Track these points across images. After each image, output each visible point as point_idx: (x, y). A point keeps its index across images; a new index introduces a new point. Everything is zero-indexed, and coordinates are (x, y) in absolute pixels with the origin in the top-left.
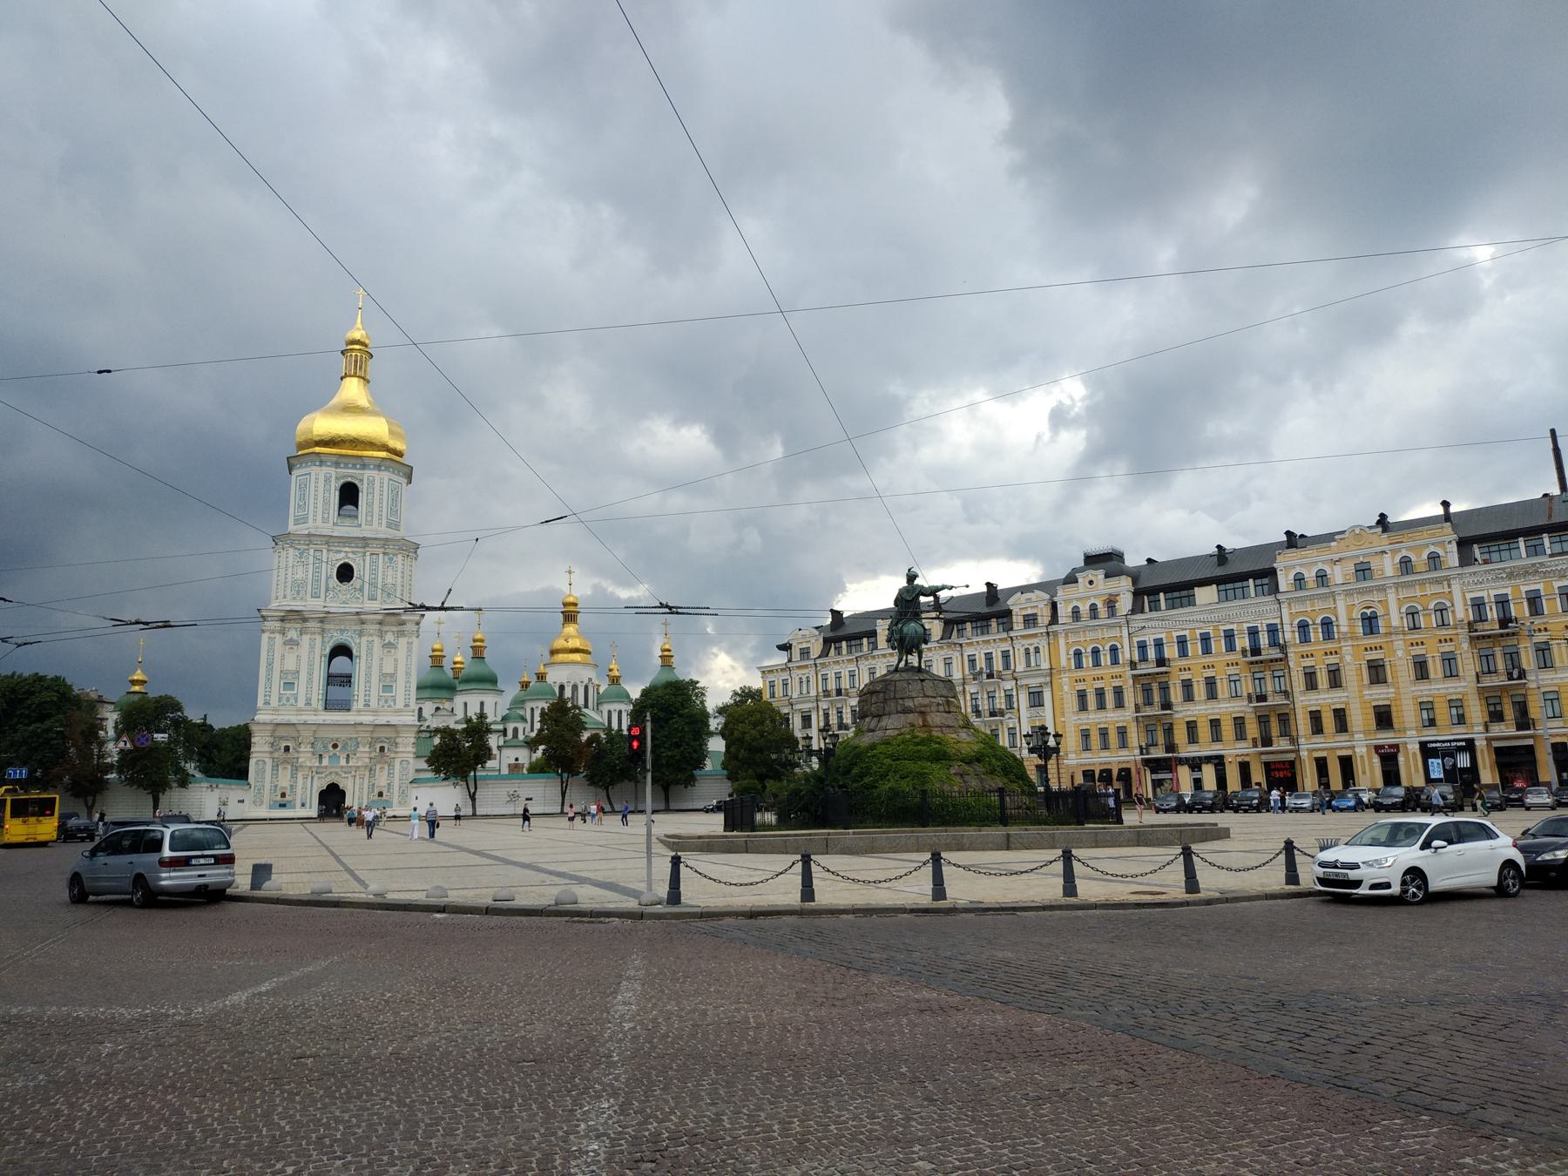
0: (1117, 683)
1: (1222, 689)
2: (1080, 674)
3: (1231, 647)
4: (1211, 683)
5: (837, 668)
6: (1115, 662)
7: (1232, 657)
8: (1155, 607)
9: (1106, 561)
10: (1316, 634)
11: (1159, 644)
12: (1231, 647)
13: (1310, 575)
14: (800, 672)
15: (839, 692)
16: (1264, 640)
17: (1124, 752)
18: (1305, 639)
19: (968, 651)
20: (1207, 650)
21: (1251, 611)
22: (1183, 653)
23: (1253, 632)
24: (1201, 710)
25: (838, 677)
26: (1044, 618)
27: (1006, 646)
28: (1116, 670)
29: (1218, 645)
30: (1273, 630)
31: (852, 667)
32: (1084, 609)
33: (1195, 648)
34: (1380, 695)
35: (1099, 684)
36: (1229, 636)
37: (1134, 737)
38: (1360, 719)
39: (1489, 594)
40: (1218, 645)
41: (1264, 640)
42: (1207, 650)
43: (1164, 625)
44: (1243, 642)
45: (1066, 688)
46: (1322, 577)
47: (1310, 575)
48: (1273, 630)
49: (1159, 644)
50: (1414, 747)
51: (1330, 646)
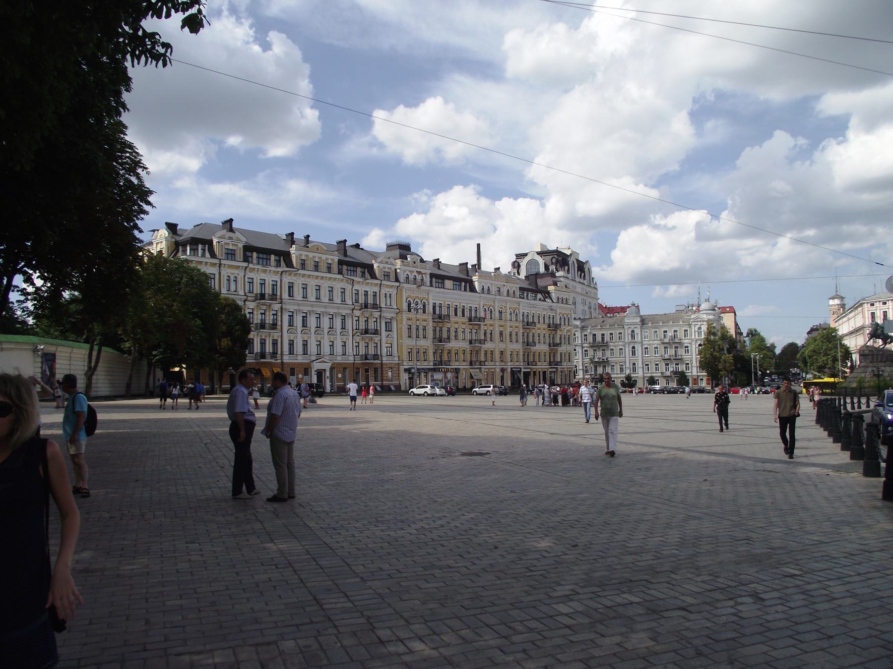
0: (424, 324)
2: (410, 315)
3: (463, 315)
5: (263, 276)
6: (424, 312)
12: (463, 315)
17: (426, 363)
19: (356, 287)
24: (453, 345)
25: (263, 284)
27: (377, 289)
28: (425, 317)
29: (459, 313)
31: (277, 278)
37: (431, 357)
38: (497, 356)
39: (526, 312)
42: (456, 315)
45: (404, 323)
50: (509, 370)
51: (491, 322)
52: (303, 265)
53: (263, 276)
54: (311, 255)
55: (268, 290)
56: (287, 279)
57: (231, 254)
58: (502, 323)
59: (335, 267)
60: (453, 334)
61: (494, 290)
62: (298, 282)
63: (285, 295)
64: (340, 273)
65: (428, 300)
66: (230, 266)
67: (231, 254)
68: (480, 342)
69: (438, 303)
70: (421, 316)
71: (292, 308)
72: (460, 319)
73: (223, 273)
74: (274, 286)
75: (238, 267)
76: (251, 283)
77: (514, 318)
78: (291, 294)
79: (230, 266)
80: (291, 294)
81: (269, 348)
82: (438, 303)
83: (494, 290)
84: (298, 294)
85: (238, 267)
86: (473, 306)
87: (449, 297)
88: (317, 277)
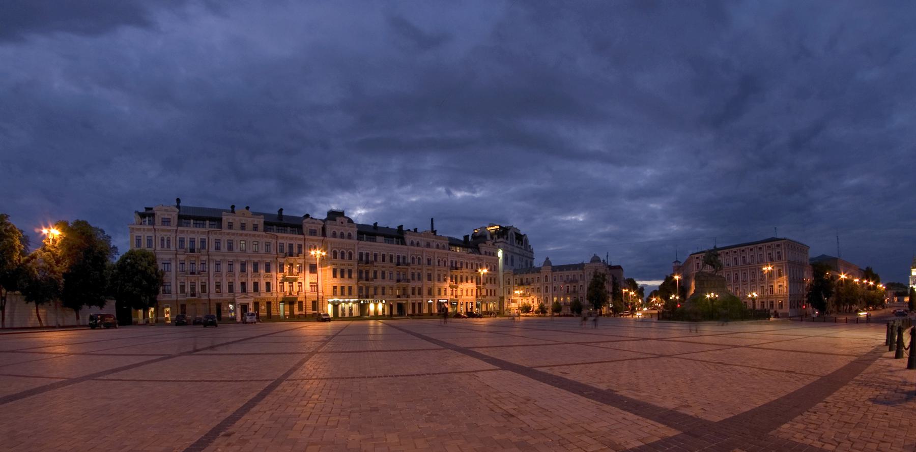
1: (387, 274)
3: (391, 261)
6: (350, 258)
7: (391, 265)
10: (416, 261)
11: (367, 255)
12: (391, 261)
13: (415, 242)
14: (163, 234)
15: (192, 250)
16: (401, 260)
18: (413, 263)
19: (280, 241)
20: (384, 260)
21: (395, 249)
22: (376, 259)
23: (398, 257)
28: (351, 262)
29: (387, 259)
30: (404, 258)
32: (338, 233)
33: (379, 258)
34: (430, 284)
35: (343, 267)
36: (391, 257)
40: (387, 259)
41: (401, 260)
42: (384, 260)
43: (367, 247)
44: (395, 260)
46: (418, 244)
47: (415, 242)
48: (404, 258)
52: (230, 226)
53: (192, 236)
54: (237, 219)
55: (198, 245)
56: (213, 237)
57: (166, 222)
58: (430, 267)
59: (261, 227)
60: (379, 275)
61: (423, 244)
62: (224, 240)
63: (212, 249)
64: (265, 231)
65: (354, 250)
66: (162, 230)
67: (166, 222)
68: (408, 281)
69: (364, 252)
70: (346, 261)
71: (218, 259)
72: (387, 263)
73: (158, 235)
74: (203, 241)
75: (169, 231)
76: (182, 241)
77: (442, 263)
78: (218, 248)
79: (162, 230)
80: (218, 248)
81: (198, 289)
82: (364, 252)
83: (423, 244)
84: (224, 247)
85: (169, 231)
86: (401, 255)
87: (380, 246)
88: (254, 235)
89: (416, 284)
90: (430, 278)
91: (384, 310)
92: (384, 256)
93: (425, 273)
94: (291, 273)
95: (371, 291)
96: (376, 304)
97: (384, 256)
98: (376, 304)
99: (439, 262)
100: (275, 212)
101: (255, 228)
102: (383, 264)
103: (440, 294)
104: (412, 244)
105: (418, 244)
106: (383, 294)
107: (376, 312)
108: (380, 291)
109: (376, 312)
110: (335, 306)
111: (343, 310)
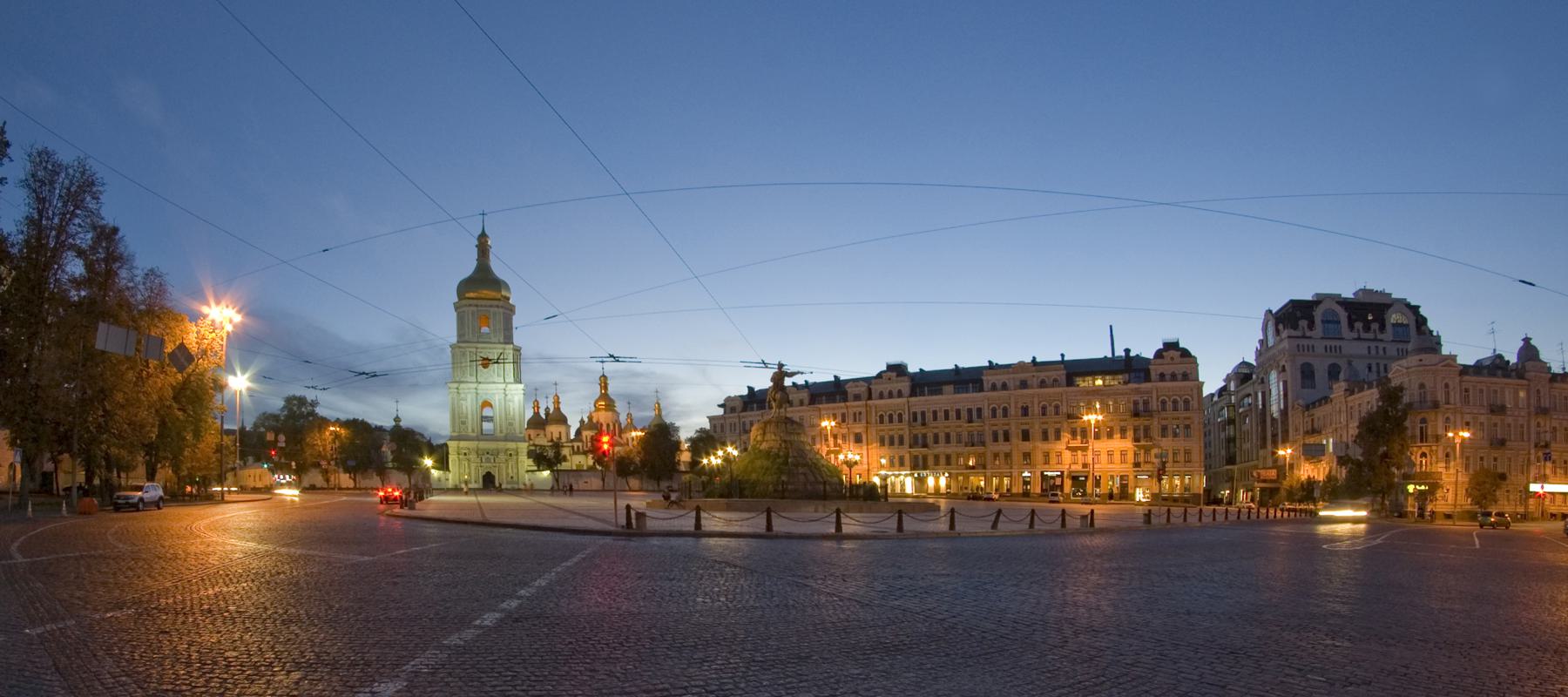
4: (948, 436)
8: (922, 394)
9: (897, 369)
11: (923, 414)
12: (958, 417)
22: (935, 418)
26: (865, 395)
29: (952, 414)
34: (1027, 446)
40: (952, 414)
43: (923, 403)
44: (964, 414)
49: (923, 414)
61: (1011, 384)
70: (896, 425)
89: (1002, 447)
90: (1026, 436)
91: (948, 487)
92: (946, 412)
93: (1015, 431)
94: (836, 445)
95: (931, 461)
96: (937, 479)
97: (946, 412)
98: (937, 479)
99: (1044, 408)
100: (745, 392)
101: (802, 403)
102: (947, 423)
103: (1047, 462)
104: (994, 387)
105: (1004, 387)
106: (948, 463)
107: (937, 489)
108: (943, 460)
109: (937, 489)
110: (884, 478)
111: (893, 485)
